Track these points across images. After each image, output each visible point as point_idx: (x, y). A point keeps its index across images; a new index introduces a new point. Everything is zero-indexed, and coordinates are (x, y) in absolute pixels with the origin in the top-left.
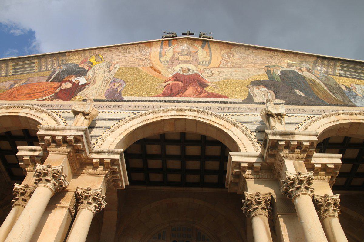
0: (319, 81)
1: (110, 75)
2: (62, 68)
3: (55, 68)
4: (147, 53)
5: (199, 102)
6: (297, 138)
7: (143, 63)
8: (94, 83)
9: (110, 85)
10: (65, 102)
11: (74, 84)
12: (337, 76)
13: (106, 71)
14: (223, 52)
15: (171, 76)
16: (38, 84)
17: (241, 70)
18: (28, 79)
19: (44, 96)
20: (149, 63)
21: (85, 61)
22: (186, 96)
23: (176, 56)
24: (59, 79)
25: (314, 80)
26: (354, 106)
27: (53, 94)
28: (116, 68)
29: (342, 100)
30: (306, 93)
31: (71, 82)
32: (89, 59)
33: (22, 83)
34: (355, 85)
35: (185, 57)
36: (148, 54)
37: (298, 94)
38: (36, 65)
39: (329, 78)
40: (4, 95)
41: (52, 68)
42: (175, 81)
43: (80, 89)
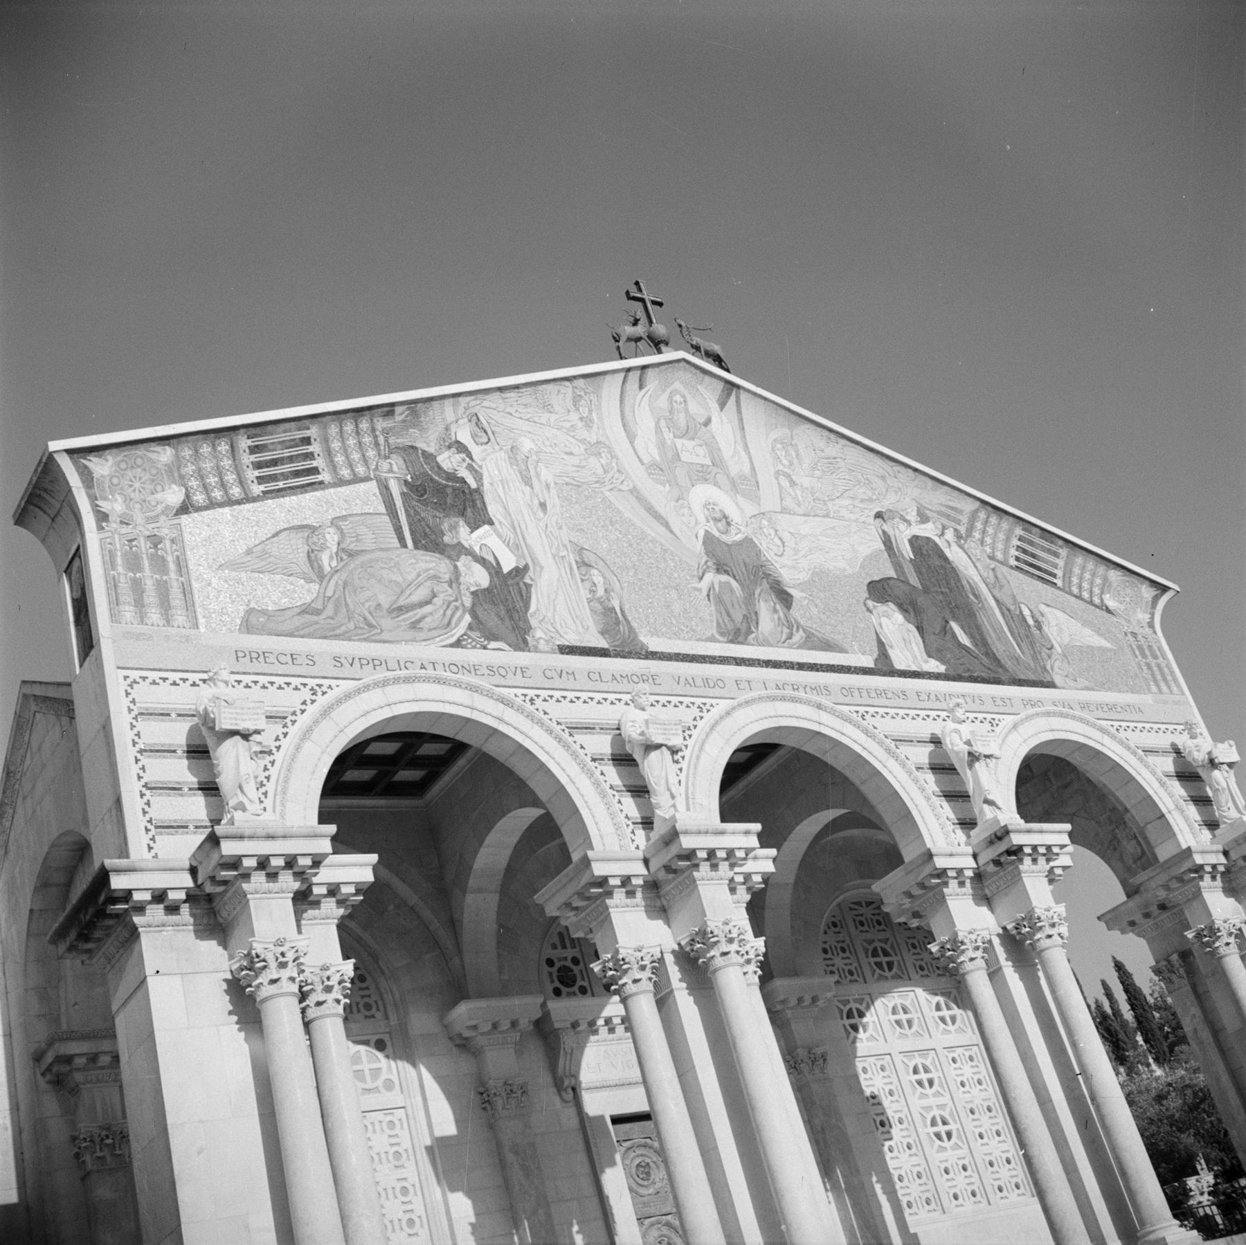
1: (554, 525)
2: (395, 468)
3: (377, 468)
4: (590, 411)
5: (801, 666)
7: (606, 472)
8: (538, 569)
9: (583, 580)
10: (520, 654)
11: (482, 561)
12: (1011, 567)
13: (532, 501)
14: (774, 435)
15: (699, 547)
16: (382, 554)
17: (833, 528)
19: (449, 624)
20: (619, 471)
22: (765, 643)
23: (668, 436)
25: (976, 583)
26: (1051, 685)
27: (464, 612)
28: (548, 486)
29: (1032, 664)
31: (469, 552)
32: (453, 428)
33: (334, 549)
35: (689, 444)
36: (596, 421)
37: (960, 639)
38: (315, 448)
39: (1000, 576)
40: (329, 611)
41: (368, 468)
42: (718, 571)
43: (520, 592)
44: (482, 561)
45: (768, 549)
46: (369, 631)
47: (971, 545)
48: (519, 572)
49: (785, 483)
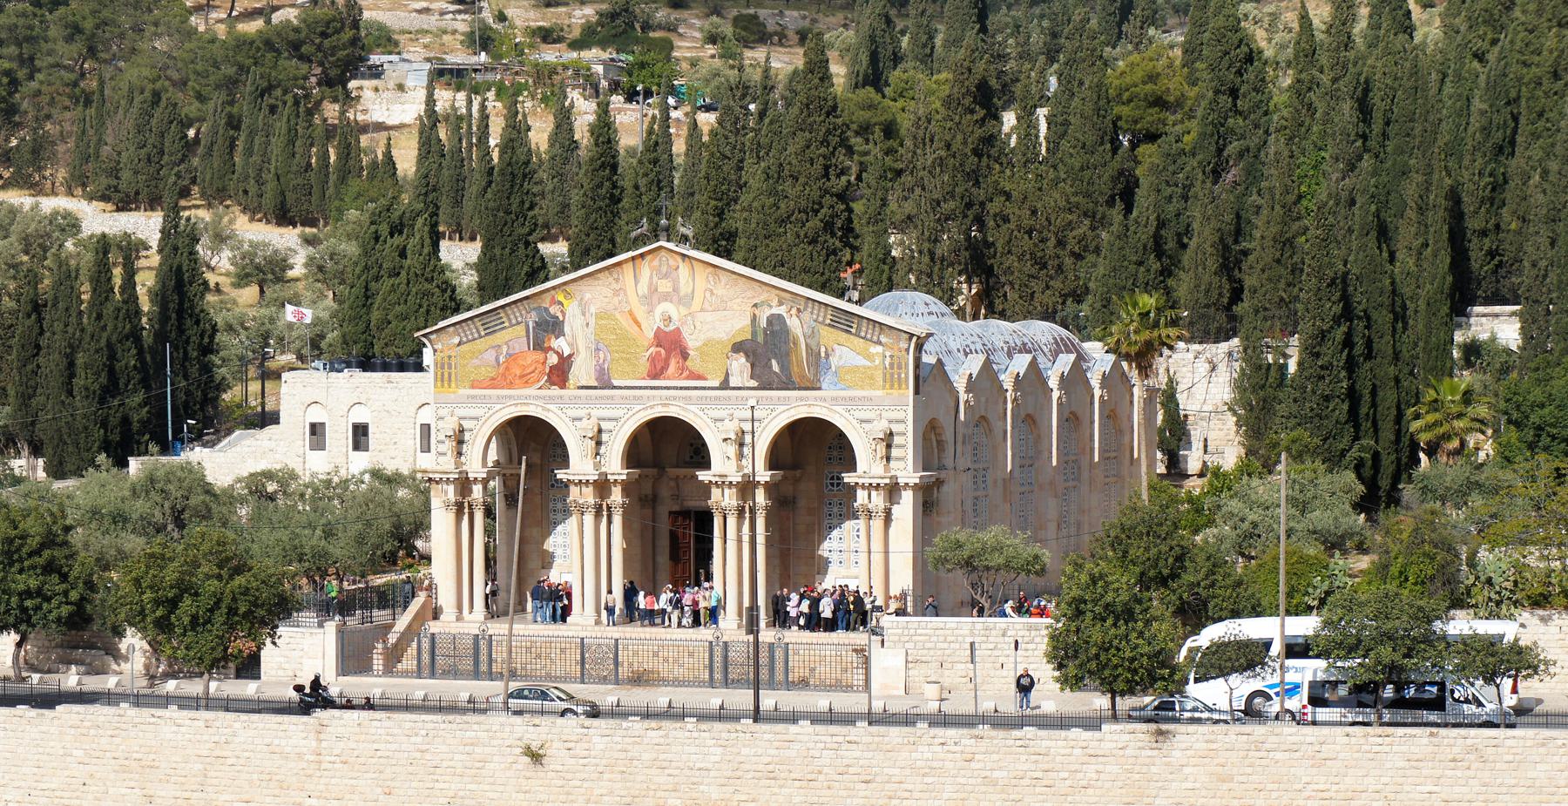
0: (802, 340)
5: (681, 388)
6: (729, 479)
11: (557, 353)
15: (651, 335)
18: (506, 343)
21: (554, 302)
22: (669, 379)
24: (540, 346)
26: (820, 389)
30: (782, 367)
31: (553, 349)
34: (836, 346)
35: (664, 281)
44: (557, 353)
45: (686, 333)
46: (511, 386)
47: (806, 316)
48: (570, 356)
49: (708, 294)
